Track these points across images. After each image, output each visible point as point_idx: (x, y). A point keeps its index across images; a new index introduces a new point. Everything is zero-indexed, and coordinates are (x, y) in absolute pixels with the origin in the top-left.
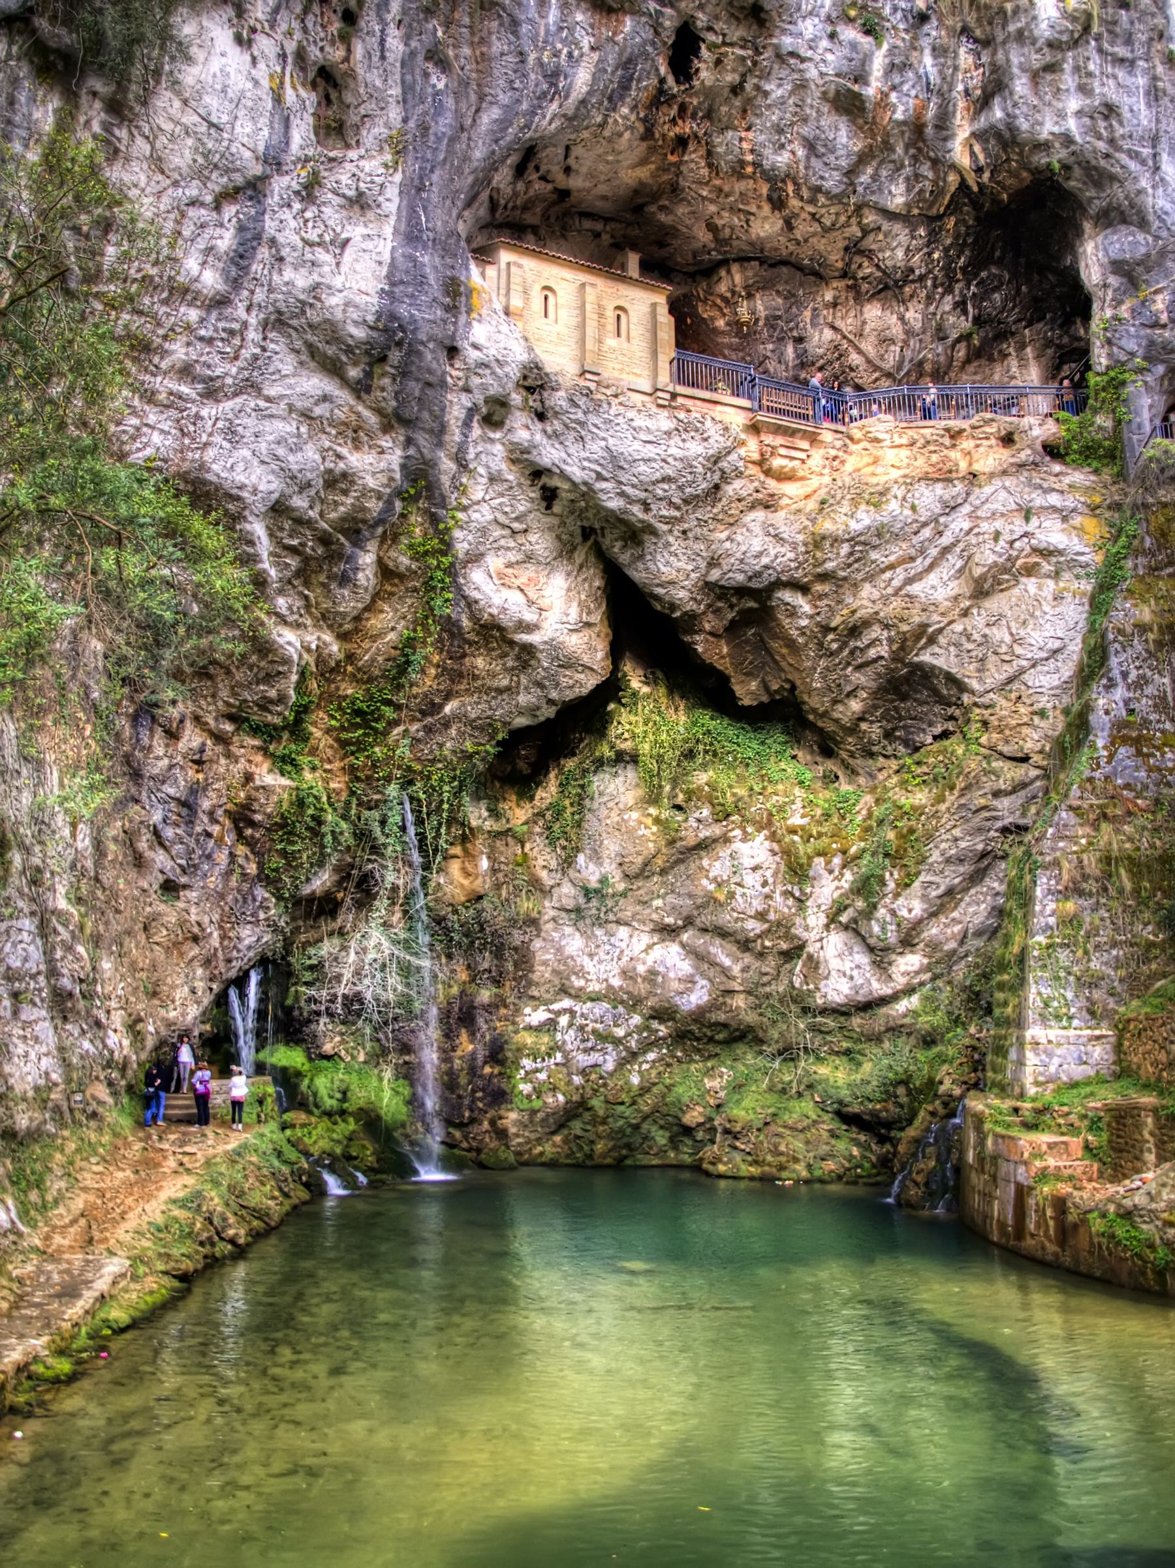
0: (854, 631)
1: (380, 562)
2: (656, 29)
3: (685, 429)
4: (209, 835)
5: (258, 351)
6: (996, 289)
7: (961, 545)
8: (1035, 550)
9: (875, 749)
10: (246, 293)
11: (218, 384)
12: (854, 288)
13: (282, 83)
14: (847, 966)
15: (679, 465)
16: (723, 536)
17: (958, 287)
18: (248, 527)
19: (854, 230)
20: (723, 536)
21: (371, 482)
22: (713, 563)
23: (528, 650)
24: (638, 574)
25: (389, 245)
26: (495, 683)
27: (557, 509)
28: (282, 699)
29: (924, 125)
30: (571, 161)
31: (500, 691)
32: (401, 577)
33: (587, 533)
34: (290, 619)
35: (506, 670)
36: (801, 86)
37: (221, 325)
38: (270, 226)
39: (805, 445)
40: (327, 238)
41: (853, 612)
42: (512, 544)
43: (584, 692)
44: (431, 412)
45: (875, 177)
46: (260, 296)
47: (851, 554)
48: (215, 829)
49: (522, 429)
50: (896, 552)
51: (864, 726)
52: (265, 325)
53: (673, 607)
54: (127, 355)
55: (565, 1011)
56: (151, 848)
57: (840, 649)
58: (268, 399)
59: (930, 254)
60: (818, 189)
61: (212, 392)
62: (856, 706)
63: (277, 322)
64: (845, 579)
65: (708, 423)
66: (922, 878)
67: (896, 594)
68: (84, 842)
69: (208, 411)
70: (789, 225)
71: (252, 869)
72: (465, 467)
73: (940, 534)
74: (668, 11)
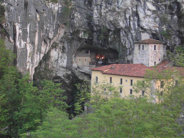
49: (79, 70)
61: (57, 71)
71: (69, 95)
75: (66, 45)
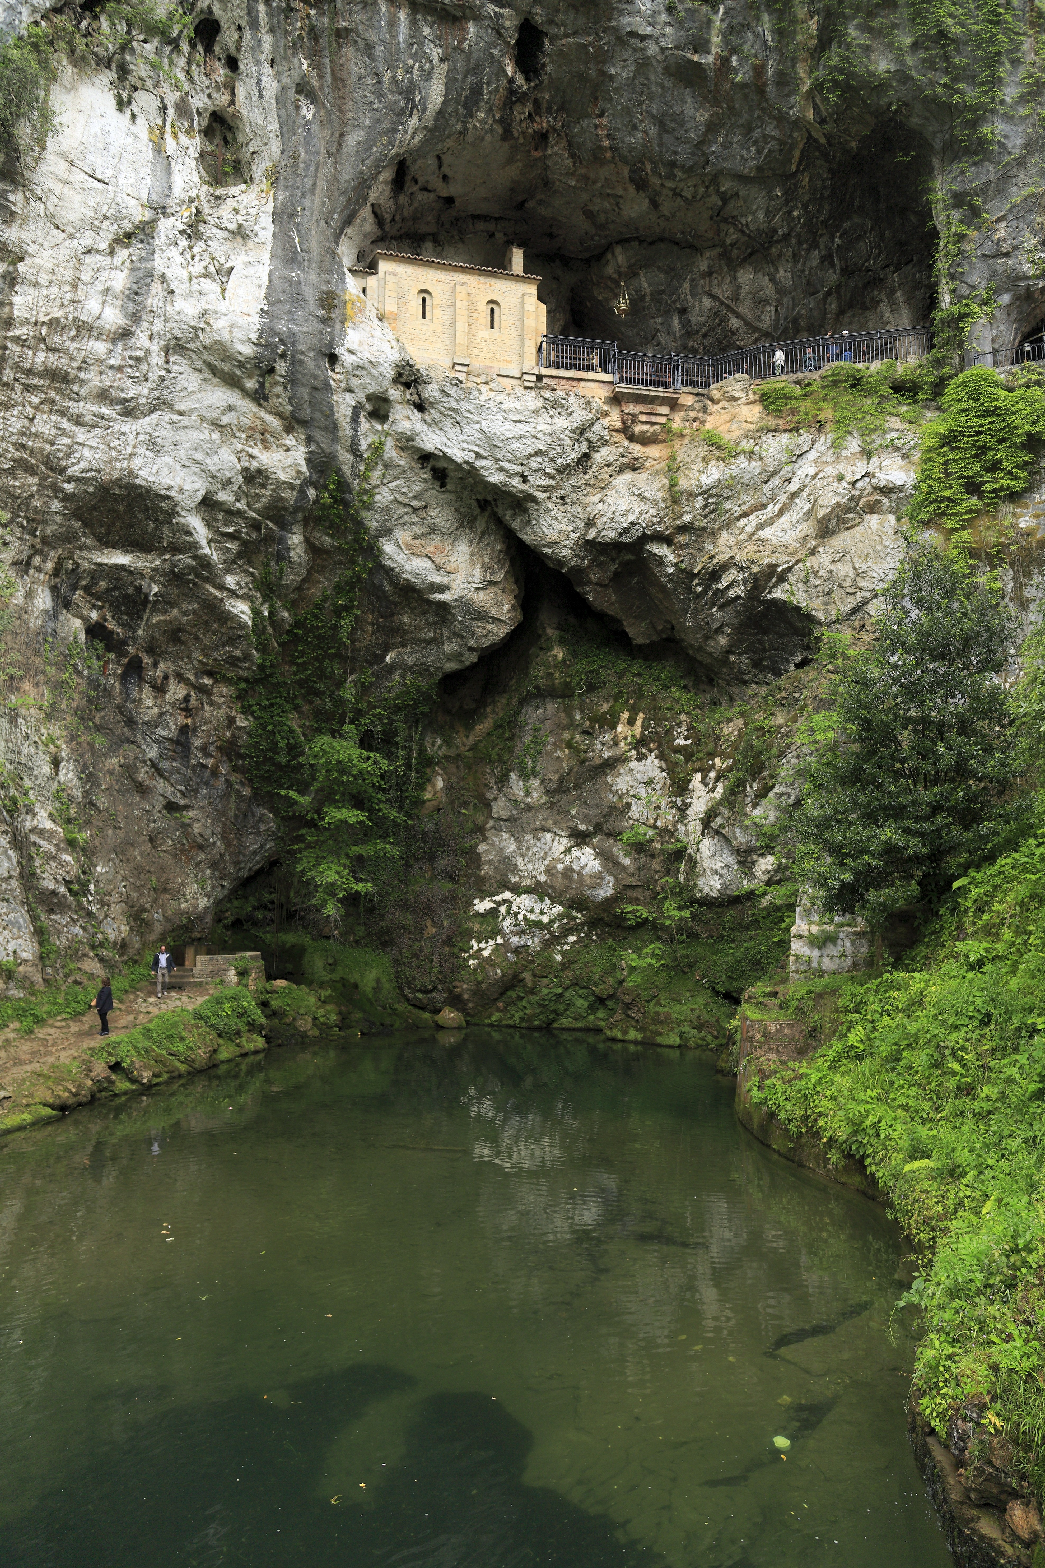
0: (715, 575)
1: (307, 540)
2: (498, 32)
3: (555, 406)
4: (204, 766)
5: (163, 373)
6: (859, 238)
7: (808, 490)
8: (876, 488)
9: (746, 677)
10: (145, 325)
11: (133, 404)
12: (725, 255)
13: (162, 134)
14: (718, 865)
15: (549, 440)
16: (596, 499)
17: (822, 241)
18: (182, 520)
19: (715, 200)
20: (596, 499)
21: (283, 477)
22: (590, 523)
23: (443, 606)
24: (527, 537)
25: (267, 269)
26: (422, 635)
27: (449, 487)
28: (247, 657)
29: (765, 84)
30: (445, 170)
31: (428, 642)
32: (327, 552)
33: (483, 505)
34: (240, 593)
35: (429, 624)
36: (644, 64)
37: (127, 354)
38: (158, 263)
39: (665, 410)
40: (212, 269)
41: (712, 558)
42: (415, 519)
43: (497, 639)
44: (322, 412)
45: (726, 145)
46: (158, 326)
47: (706, 506)
48: (210, 762)
49: (405, 419)
50: (748, 500)
51: (732, 658)
52: (167, 350)
53: (560, 563)
54: (49, 387)
55: (505, 901)
56: (152, 778)
57: (705, 592)
58: (181, 414)
59: (790, 213)
60: (673, 164)
61: (129, 410)
62: (723, 641)
63: (176, 347)
64: (703, 529)
65: (572, 399)
66: (775, 790)
67: (749, 539)
68: (68, 774)
69: (128, 426)
70: (655, 204)
71: (247, 792)
72: (361, 456)
73: (789, 480)
74: (506, 11)
75: (260, 97)
